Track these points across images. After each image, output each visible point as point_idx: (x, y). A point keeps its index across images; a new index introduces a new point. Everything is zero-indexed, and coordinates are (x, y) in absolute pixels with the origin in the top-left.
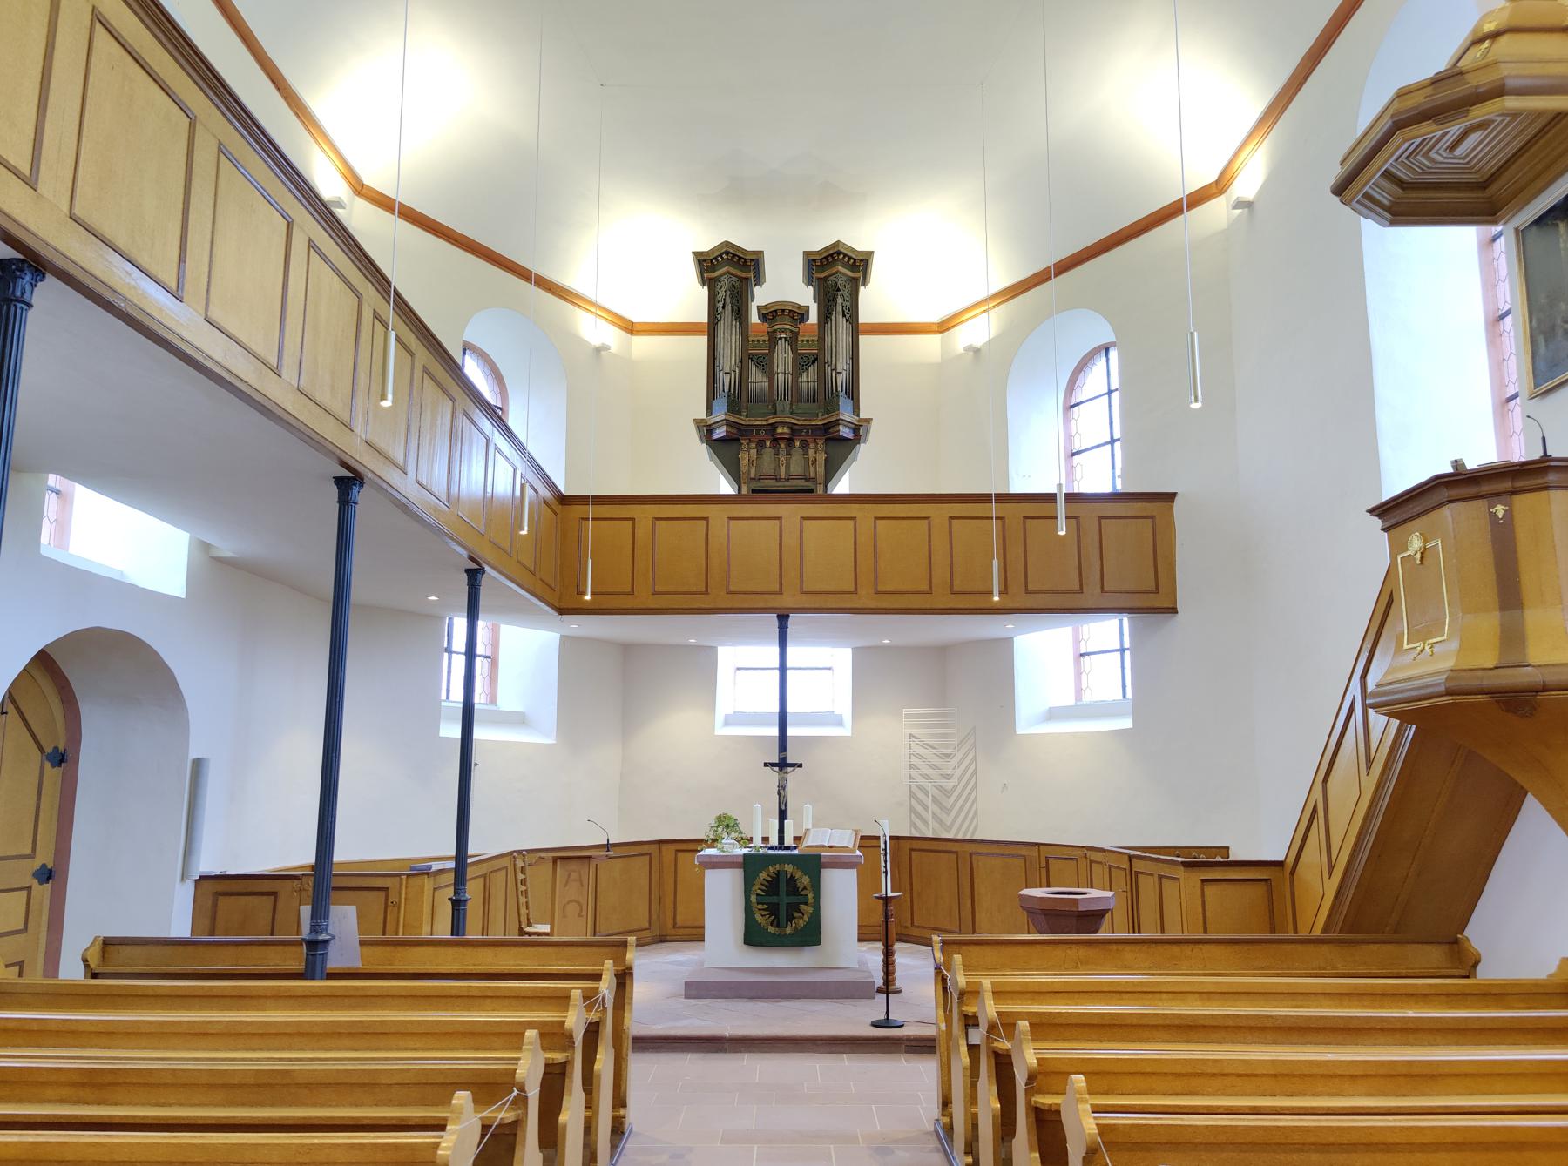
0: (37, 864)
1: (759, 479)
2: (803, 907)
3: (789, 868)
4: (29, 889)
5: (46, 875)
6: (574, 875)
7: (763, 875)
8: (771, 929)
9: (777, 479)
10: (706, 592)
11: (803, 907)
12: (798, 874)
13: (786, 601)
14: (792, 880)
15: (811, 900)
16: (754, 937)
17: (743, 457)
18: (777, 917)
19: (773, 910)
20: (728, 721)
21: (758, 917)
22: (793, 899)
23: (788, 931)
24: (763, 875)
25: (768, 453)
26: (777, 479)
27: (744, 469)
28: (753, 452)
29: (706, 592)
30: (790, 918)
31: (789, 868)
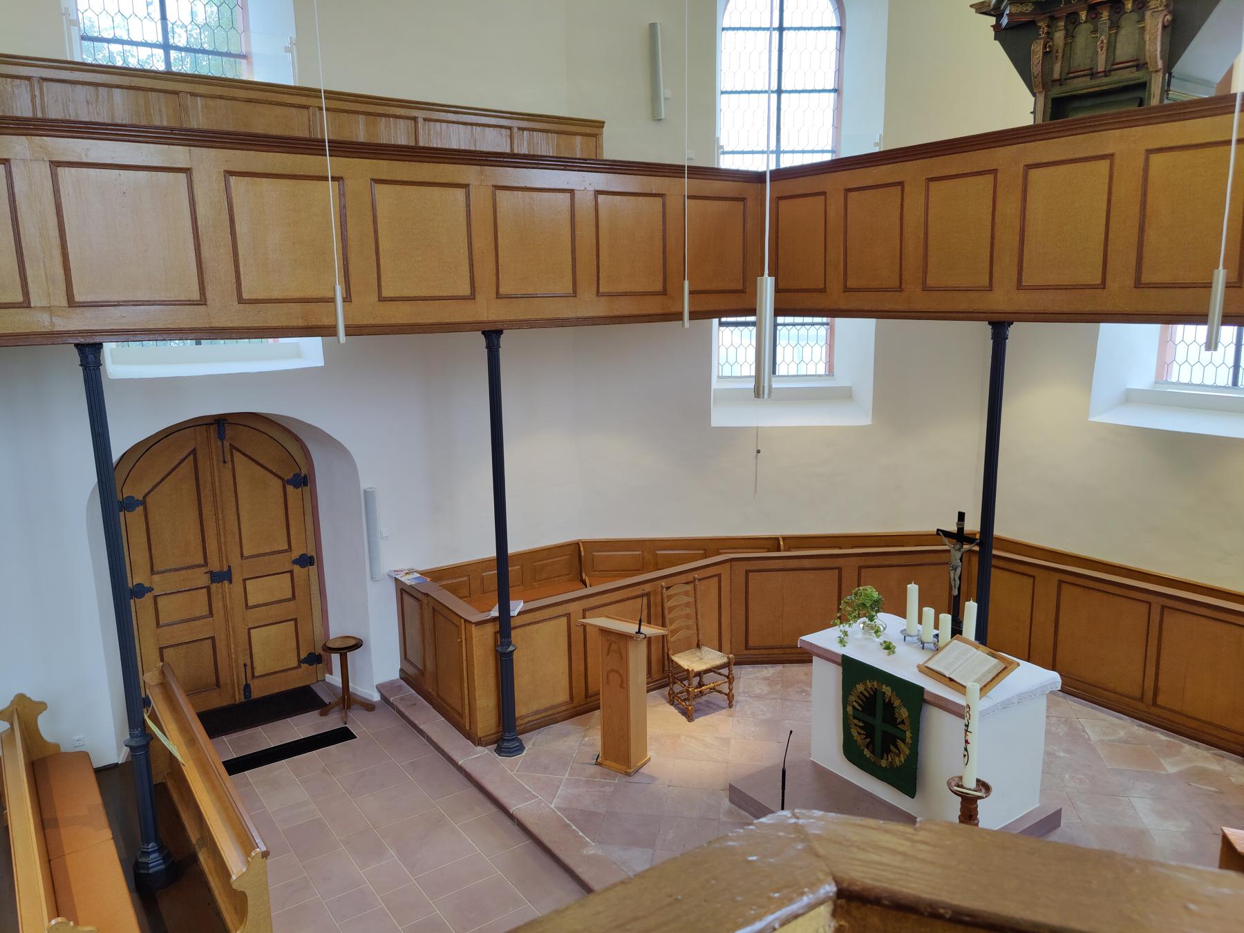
0: (296, 554)
1: (1060, 82)
2: (900, 743)
3: (887, 690)
4: (291, 572)
5: (306, 561)
6: (614, 647)
7: (860, 687)
8: (867, 753)
9: (1093, 74)
10: (900, 289)
11: (900, 743)
12: (897, 703)
13: (1000, 300)
14: (889, 707)
15: (909, 740)
16: (851, 752)
17: (1037, 49)
18: (872, 742)
19: (869, 730)
20: (1130, 398)
21: (854, 732)
22: (889, 729)
23: (884, 763)
24: (860, 687)
25: (1084, 30)
26: (1093, 74)
27: (1036, 69)
28: (1059, 36)
29: (900, 289)
30: (886, 751)
31: (887, 690)
